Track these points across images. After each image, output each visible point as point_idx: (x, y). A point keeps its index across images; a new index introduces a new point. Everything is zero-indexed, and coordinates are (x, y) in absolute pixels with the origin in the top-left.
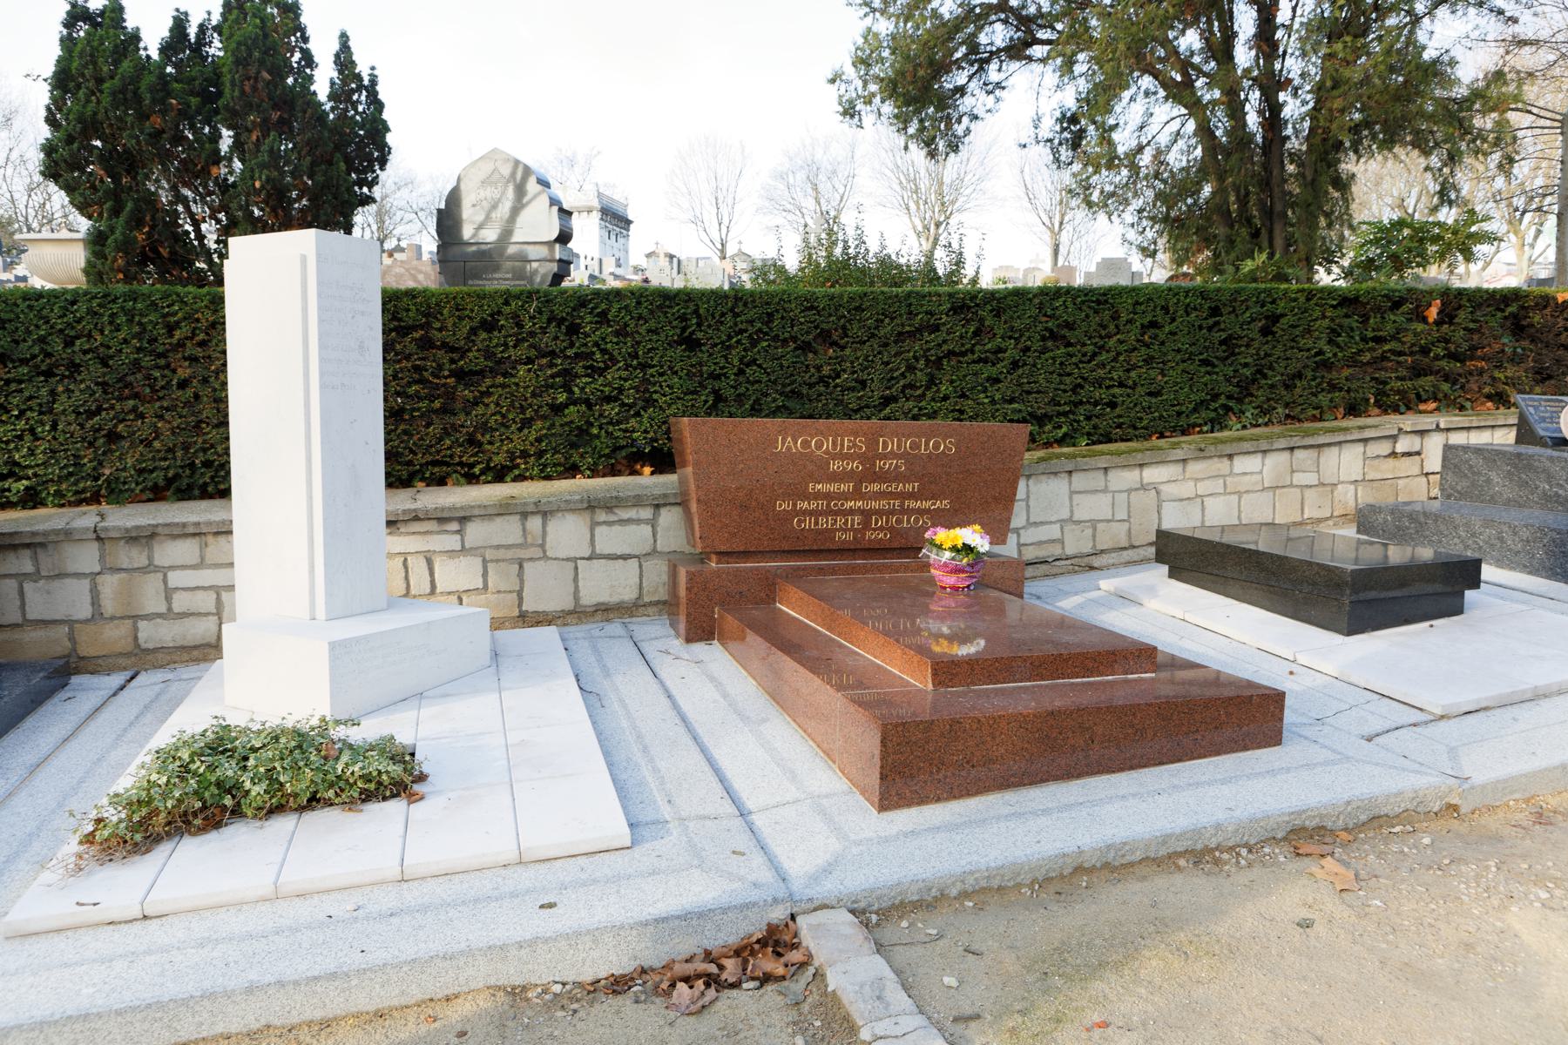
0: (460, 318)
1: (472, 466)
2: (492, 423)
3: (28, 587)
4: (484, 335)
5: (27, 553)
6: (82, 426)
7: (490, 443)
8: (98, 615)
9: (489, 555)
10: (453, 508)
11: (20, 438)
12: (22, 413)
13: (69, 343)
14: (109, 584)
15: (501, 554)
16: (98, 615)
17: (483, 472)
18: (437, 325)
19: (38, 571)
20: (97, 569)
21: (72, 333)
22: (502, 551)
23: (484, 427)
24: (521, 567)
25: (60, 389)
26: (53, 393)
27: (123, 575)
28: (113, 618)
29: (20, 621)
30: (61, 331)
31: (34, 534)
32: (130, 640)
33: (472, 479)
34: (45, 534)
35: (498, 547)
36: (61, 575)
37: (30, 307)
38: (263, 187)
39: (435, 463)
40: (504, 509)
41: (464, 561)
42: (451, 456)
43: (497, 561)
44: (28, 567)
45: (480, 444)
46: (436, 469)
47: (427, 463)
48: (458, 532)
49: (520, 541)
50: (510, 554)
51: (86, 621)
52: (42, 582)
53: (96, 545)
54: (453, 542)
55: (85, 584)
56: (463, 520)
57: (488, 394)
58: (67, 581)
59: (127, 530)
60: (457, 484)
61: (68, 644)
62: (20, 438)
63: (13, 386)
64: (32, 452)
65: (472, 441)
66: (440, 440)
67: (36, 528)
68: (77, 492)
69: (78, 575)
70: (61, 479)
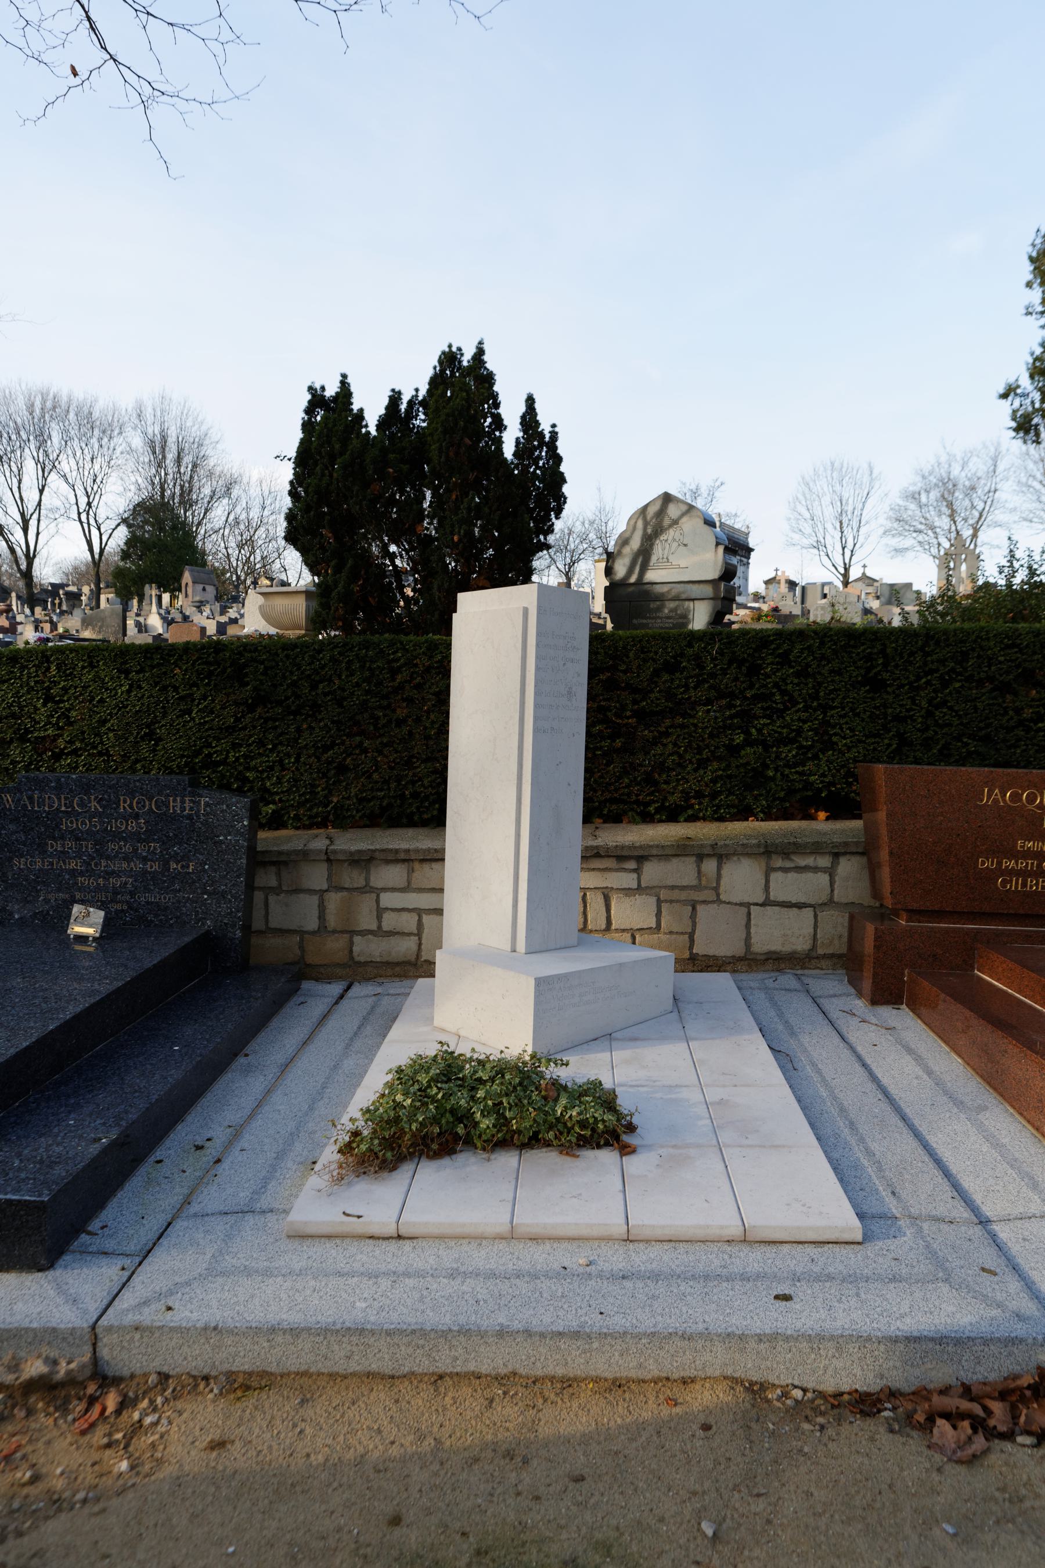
0: (645, 661)
1: (648, 804)
2: (669, 763)
3: (272, 899)
4: (666, 677)
5: (273, 869)
6: (319, 759)
7: (667, 782)
8: (322, 928)
9: (664, 894)
10: (633, 847)
11: (272, 768)
12: (275, 746)
13: (314, 687)
14: (333, 900)
15: (676, 895)
16: (322, 928)
17: (658, 811)
18: (623, 667)
19: (280, 885)
20: (325, 887)
21: (317, 678)
22: (677, 891)
23: (661, 767)
24: (694, 909)
25: (305, 726)
26: (299, 730)
27: (345, 894)
28: (334, 932)
29: (263, 928)
30: (309, 676)
31: (280, 853)
32: (346, 952)
33: (647, 818)
34: (289, 853)
35: (673, 888)
36: (298, 891)
37: (287, 657)
38: (460, 540)
39: (613, 801)
40: (682, 850)
41: (639, 899)
42: (629, 795)
43: (671, 901)
44: (273, 882)
45: (656, 783)
46: (614, 807)
47: (606, 801)
48: (635, 870)
49: (694, 882)
50: (683, 895)
51: (313, 933)
52: (283, 895)
53: (325, 865)
54: (628, 880)
55: (315, 899)
56: (641, 859)
57: (667, 734)
58: (301, 896)
59: (351, 854)
60: (632, 821)
61: (298, 952)
62: (272, 768)
63: (270, 724)
64: (279, 781)
65: (649, 780)
66: (620, 778)
67: (285, 847)
68: (310, 817)
69: (311, 892)
70: (301, 804)
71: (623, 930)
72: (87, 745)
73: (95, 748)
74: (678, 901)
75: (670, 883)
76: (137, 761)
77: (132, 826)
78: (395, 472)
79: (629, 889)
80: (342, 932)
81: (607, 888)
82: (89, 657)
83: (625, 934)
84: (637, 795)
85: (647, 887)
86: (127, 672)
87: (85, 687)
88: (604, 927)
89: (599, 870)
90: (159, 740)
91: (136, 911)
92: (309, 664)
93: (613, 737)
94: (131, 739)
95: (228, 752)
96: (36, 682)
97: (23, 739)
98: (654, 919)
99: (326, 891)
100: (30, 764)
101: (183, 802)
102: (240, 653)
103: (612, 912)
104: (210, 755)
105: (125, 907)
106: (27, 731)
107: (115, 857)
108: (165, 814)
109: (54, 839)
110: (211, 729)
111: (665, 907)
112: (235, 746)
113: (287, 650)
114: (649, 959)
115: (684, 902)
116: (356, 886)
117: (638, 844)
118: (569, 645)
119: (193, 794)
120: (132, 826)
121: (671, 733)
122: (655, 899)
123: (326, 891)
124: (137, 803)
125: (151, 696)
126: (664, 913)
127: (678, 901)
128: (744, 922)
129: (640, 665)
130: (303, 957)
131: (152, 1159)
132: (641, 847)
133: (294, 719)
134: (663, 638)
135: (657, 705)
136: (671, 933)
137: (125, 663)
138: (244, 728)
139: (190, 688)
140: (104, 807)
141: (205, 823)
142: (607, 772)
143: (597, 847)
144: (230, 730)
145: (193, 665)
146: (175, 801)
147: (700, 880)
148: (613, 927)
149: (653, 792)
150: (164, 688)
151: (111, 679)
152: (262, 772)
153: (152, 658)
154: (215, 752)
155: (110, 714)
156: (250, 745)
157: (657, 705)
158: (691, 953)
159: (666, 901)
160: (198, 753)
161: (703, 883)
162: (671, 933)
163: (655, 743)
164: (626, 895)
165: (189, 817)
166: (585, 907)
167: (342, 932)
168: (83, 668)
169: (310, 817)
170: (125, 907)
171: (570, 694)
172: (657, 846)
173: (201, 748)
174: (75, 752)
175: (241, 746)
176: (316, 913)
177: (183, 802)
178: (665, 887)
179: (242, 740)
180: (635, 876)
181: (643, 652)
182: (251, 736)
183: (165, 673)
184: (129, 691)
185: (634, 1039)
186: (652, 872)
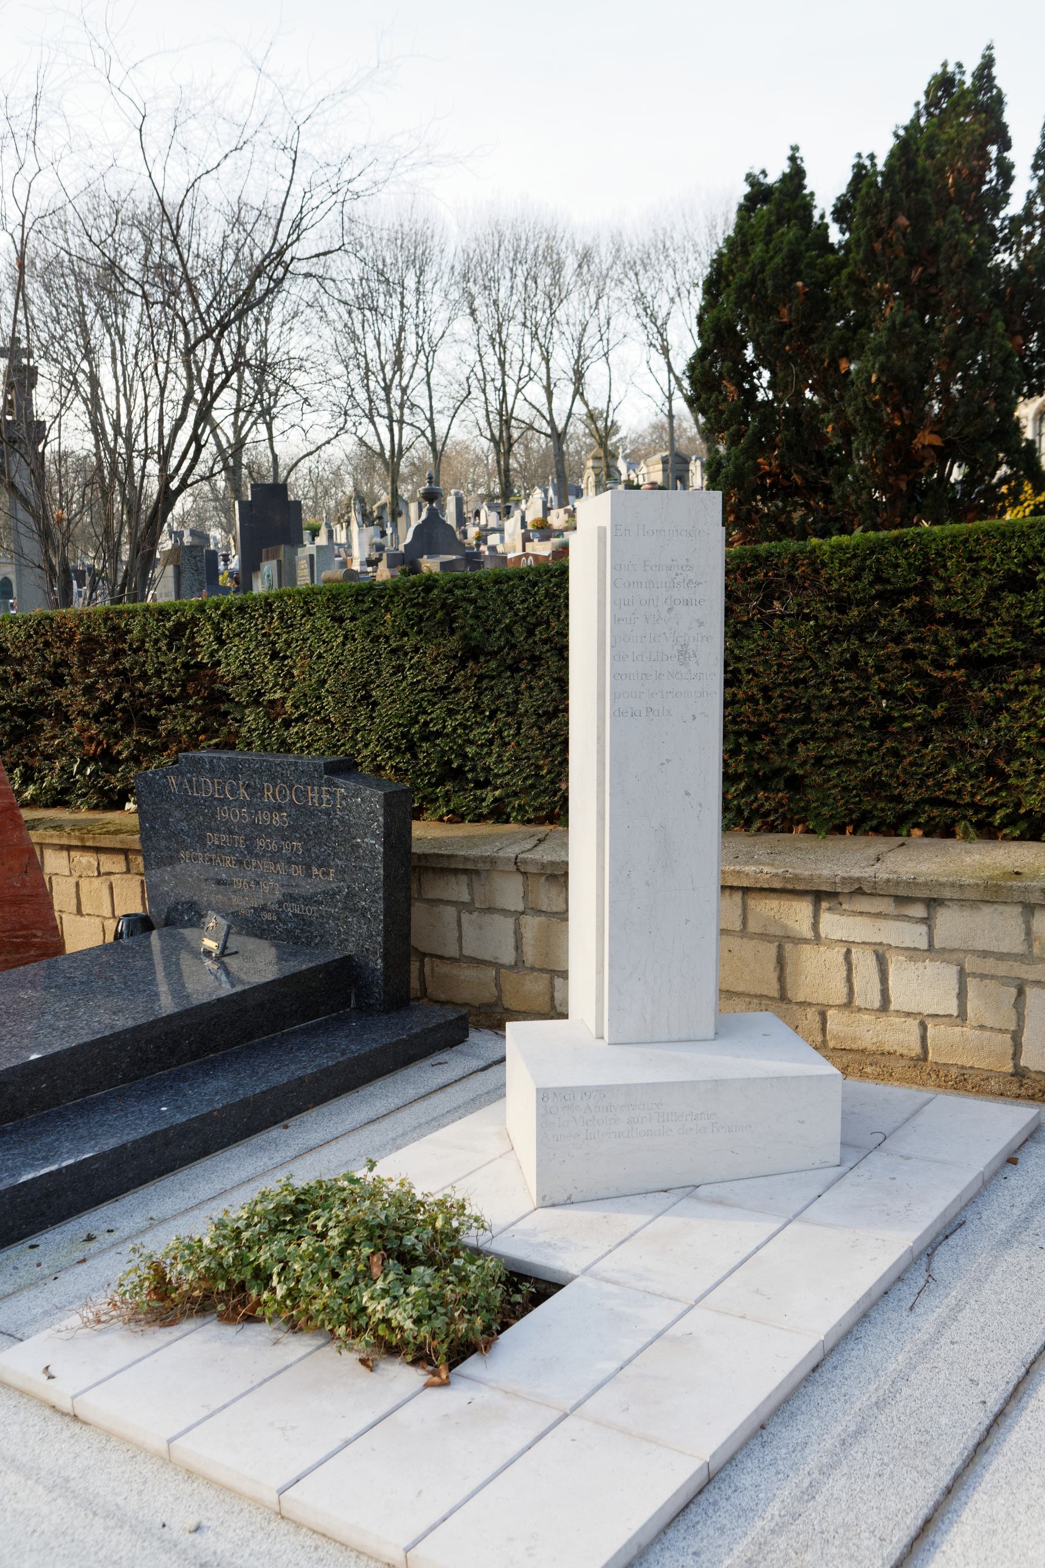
0: (975, 573)
1: (993, 809)
2: (1021, 743)
3: (465, 917)
4: (1011, 599)
5: (464, 879)
6: (541, 729)
7: (1022, 775)
8: (519, 964)
9: (971, 964)
10: (913, 883)
11: (491, 742)
12: (493, 713)
13: (531, 633)
14: (531, 925)
15: (989, 966)
16: (519, 964)
17: (1011, 820)
18: (938, 586)
19: (473, 899)
20: (521, 907)
21: (533, 620)
22: (991, 961)
23: (1012, 752)
24: (1021, 992)
25: (523, 686)
26: (517, 692)
27: (543, 919)
28: (533, 969)
29: (457, 956)
30: (524, 618)
31: (466, 859)
32: (547, 998)
33: (987, 831)
34: (476, 860)
35: (985, 954)
36: (491, 910)
37: (500, 592)
38: (878, 380)
39: (935, 802)
40: (992, 893)
41: (931, 968)
42: (959, 792)
43: (983, 977)
44: (466, 898)
45: (1002, 776)
46: (936, 812)
47: (924, 801)
48: (924, 921)
49: (1020, 949)
50: (1002, 969)
51: (511, 968)
52: (476, 914)
53: (519, 878)
54: (914, 935)
55: (510, 922)
56: (933, 903)
57: (1016, 695)
58: (496, 917)
59: (543, 866)
60: (966, 837)
61: (494, 991)
62: (491, 742)
63: (485, 684)
64: (500, 761)
65: (991, 769)
66: (944, 765)
67: (475, 852)
68: (536, 810)
69: (505, 912)
70: (526, 790)
71: (908, 1014)
72: (311, 710)
73: (319, 713)
74: (992, 977)
75: (980, 945)
76: (357, 731)
77: (277, 820)
78: (806, 285)
79: (915, 949)
80: (542, 970)
81: (881, 944)
82: (306, 603)
83: (910, 1021)
84: (973, 795)
85: (943, 949)
86: (341, 620)
87: (305, 640)
88: (877, 1005)
89: (868, 914)
90: (375, 704)
91: (285, 924)
92: (523, 602)
93: (932, 700)
94: (349, 703)
95: (445, 721)
96: (264, 635)
97: (257, 703)
98: (955, 1003)
99: (523, 913)
100: (264, 733)
101: (320, 793)
102: (450, 591)
103: (890, 983)
104: (426, 724)
105: (275, 918)
106: (261, 694)
107: (263, 856)
108: (304, 806)
109: (211, 830)
110: (423, 690)
111: (971, 983)
112: (451, 713)
113: (501, 583)
114: (780, 1079)
115: (1004, 980)
116: (555, 909)
117: (921, 880)
118: (680, 578)
119: (330, 783)
120: (277, 820)
121: (1024, 693)
122: (952, 971)
123: (523, 913)
124: (280, 792)
125: (363, 650)
126: (970, 994)
127: (992, 977)
128: (483, 1074)
129: (965, 582)
130: (499, 998)
131: (30, 1243)
132: (925, 884)
133: (512, 677)
134: (1003, 535)
135: (1000, 646)
136: (982, 1027)
137: (337, 609)
138: (457, 690)
139: (401, 639)
140: (251, 795)
141: (342, 821)
142: (923, 756)
143: (859, 880)
144: (442, 691)
145: (404, 608)
146: (312, 790)
147: (1030, 946)
148: (892, 1007)
149: (1000, 789)
150: (375, 640)
151: (327, 629)
152: (482, 746)
153: (363, 601)
154: (432, 720)
155: (328, 672)
156: (465, 711)
157: (1000, 646)
158: (1016, 1066)
159: (974, 975)
160: (415, 721)
161: (1036, 950)
162: (982, 1027)
163: (999, 708)
164: (911, 959)
165: (327, 812)
166: (850, 970)
167: (542, 970)
168: (303, 616)
169: (536, 810)
170: (275, 918)
171: (684, 654)
172: (953, 885)
173: (417, 715)
174: (301, 718)
175: (457, 712)
176: (511, 941)
177: (320, 793)
178: (974, 952)
179: (458, 704)
180: (923, 929)
181: (970, 560)
182: (466, 700)
183: (374, 620)
184: (344, 644)
185: (719, 1202)
186: (950, 924)
